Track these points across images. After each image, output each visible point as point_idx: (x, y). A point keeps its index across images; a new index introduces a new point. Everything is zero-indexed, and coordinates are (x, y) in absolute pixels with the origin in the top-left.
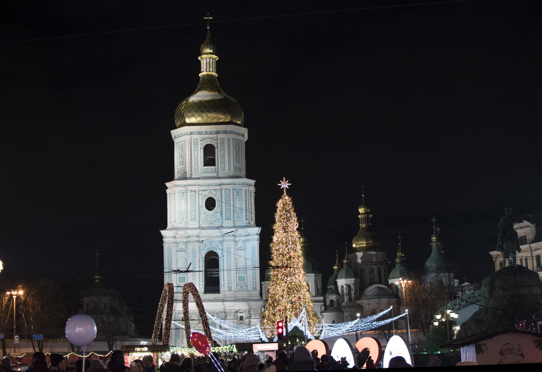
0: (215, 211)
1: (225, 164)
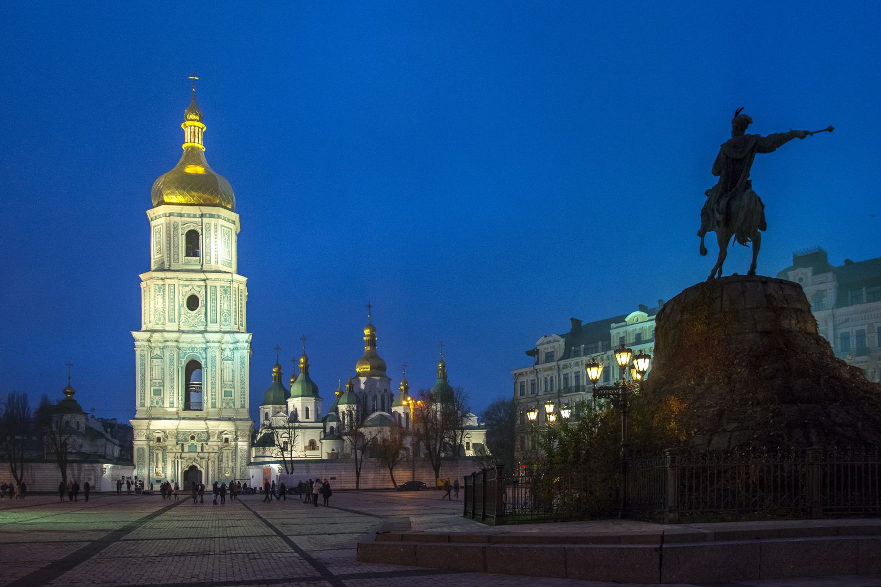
0: (198, 312)
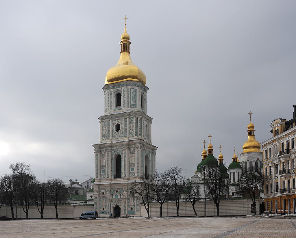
0: (120, 132)
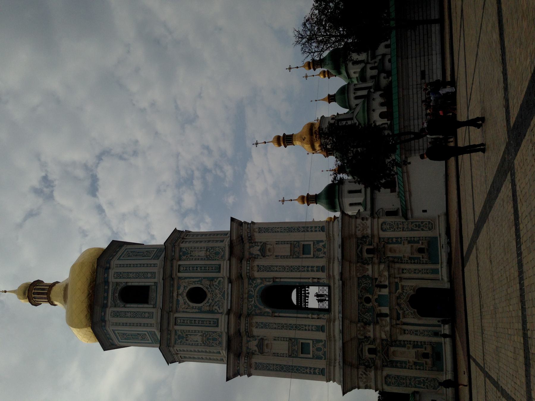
0: (207, 288)
1: (146, 272)
